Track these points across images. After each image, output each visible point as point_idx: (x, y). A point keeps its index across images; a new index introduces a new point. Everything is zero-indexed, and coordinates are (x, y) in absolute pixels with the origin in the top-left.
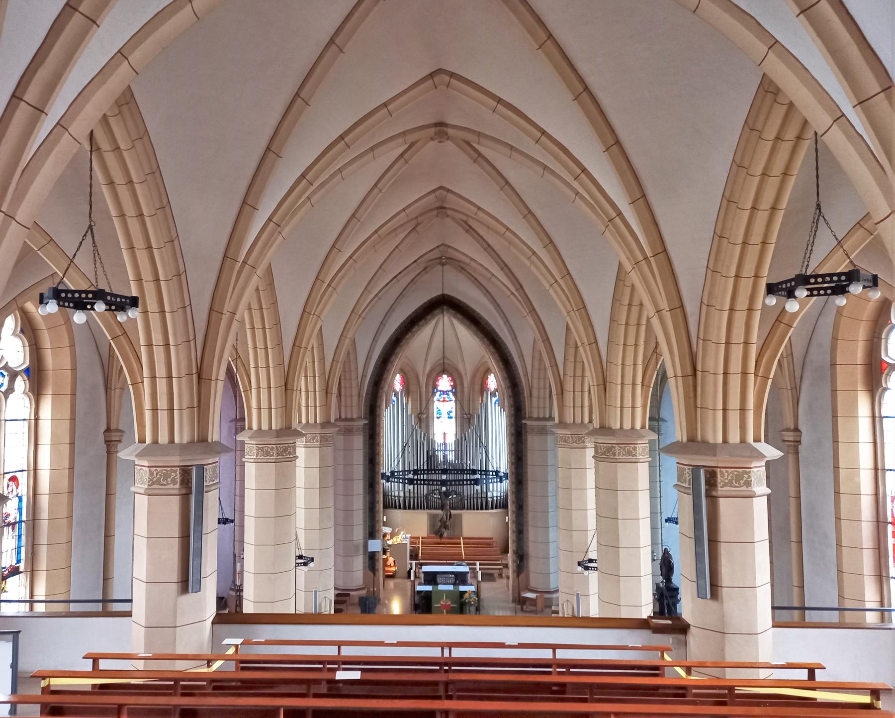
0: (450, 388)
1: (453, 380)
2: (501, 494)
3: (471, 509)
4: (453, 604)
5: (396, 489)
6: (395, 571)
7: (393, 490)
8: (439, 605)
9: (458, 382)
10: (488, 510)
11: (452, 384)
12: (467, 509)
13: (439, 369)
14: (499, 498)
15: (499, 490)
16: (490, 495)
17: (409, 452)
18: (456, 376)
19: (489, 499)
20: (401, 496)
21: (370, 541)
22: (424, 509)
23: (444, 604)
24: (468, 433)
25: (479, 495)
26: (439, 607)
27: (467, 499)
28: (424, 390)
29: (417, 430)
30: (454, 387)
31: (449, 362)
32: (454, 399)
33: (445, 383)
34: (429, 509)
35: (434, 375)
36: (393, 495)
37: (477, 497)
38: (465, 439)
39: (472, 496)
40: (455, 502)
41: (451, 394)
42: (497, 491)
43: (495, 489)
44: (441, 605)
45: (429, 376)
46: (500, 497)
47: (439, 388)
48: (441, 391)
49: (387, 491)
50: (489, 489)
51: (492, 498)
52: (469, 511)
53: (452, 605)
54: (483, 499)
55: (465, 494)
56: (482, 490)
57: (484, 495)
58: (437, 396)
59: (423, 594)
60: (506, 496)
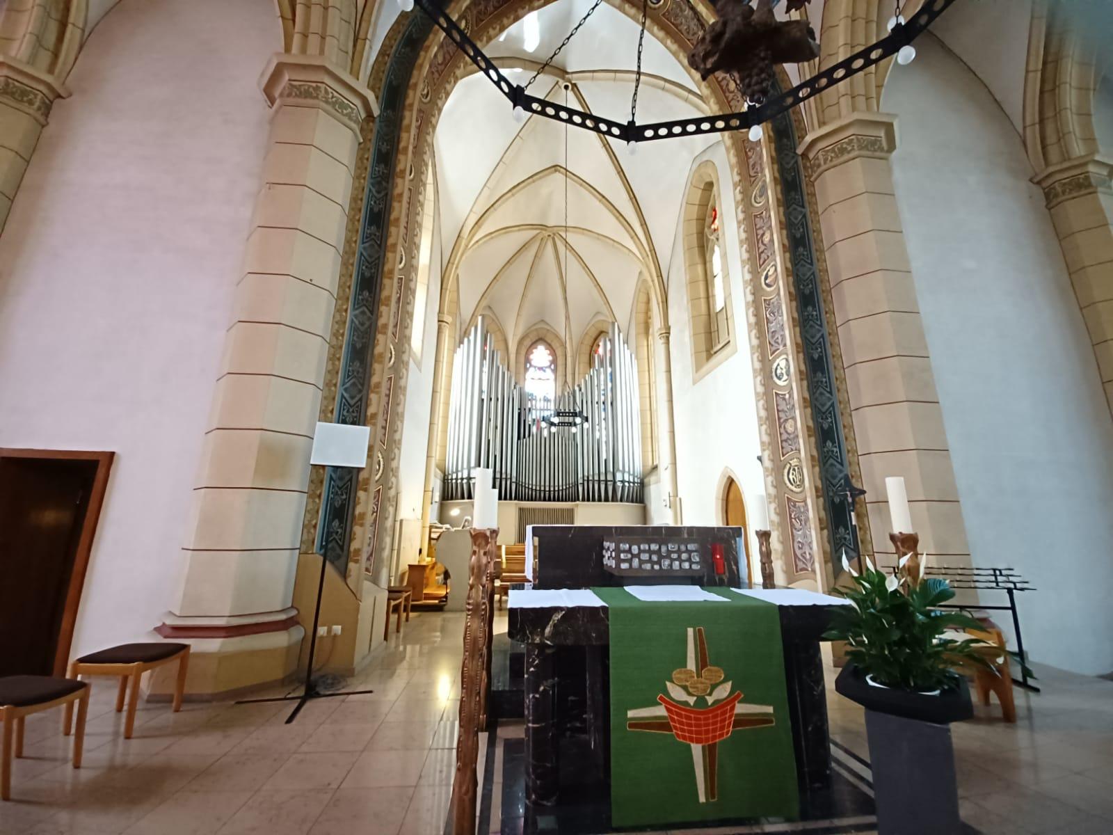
0: (548, 364)
1: (553, 352)
2: (634, 479)
3: (588, 500)
4: (745, 701)
5: (465, 466)
6: (446, 597)
7: (460, 469)
8: (660, 711)
9: (559, 352)
10: (617, 501)
11: (551, 358)
12: (583, 500)
13: (533, 337)
14: (632, 484)
15: (631, 472)
16: (619, 477)
17: (490, 420)
18: (555, 345)
19: (619, 484)
20: (472, 476)
21: (318, 423)
22: (511, 499)
23: (692, 700)
24: (586, 381)
25: (603, 478)
26: (660, 724)
27: (583, 484)
28: (513, 357)
29: (504, 374)
30: (554, 362)
31: (549, 328)
32: (552, 376)
33: (541, 355)
34: (519, 500)
35: (527, 342)
36: (460, 476)
37: (599, 481)
38: (580, 390)
39: (591, 478)
40: (562, 490)
41: (548, 371)
42: (629, 472)
43: (627, 469)
44: (671, 704)
45: (520, 343)
46: (634, 483)
47: (533, 363)
48: (535, 367)
49: (450, 472)
50: (618, 470)
51: (623, 482)
52: (586, 503)
53: (741, 708)
54: (609, 483)
55: (580, 475)
56: (608, 470)
57: (610, 477)
58: (531, 373)
59: (548, 630)
60: (640, 483)
